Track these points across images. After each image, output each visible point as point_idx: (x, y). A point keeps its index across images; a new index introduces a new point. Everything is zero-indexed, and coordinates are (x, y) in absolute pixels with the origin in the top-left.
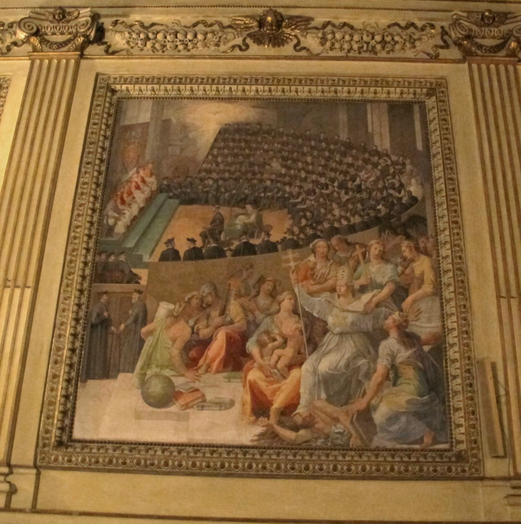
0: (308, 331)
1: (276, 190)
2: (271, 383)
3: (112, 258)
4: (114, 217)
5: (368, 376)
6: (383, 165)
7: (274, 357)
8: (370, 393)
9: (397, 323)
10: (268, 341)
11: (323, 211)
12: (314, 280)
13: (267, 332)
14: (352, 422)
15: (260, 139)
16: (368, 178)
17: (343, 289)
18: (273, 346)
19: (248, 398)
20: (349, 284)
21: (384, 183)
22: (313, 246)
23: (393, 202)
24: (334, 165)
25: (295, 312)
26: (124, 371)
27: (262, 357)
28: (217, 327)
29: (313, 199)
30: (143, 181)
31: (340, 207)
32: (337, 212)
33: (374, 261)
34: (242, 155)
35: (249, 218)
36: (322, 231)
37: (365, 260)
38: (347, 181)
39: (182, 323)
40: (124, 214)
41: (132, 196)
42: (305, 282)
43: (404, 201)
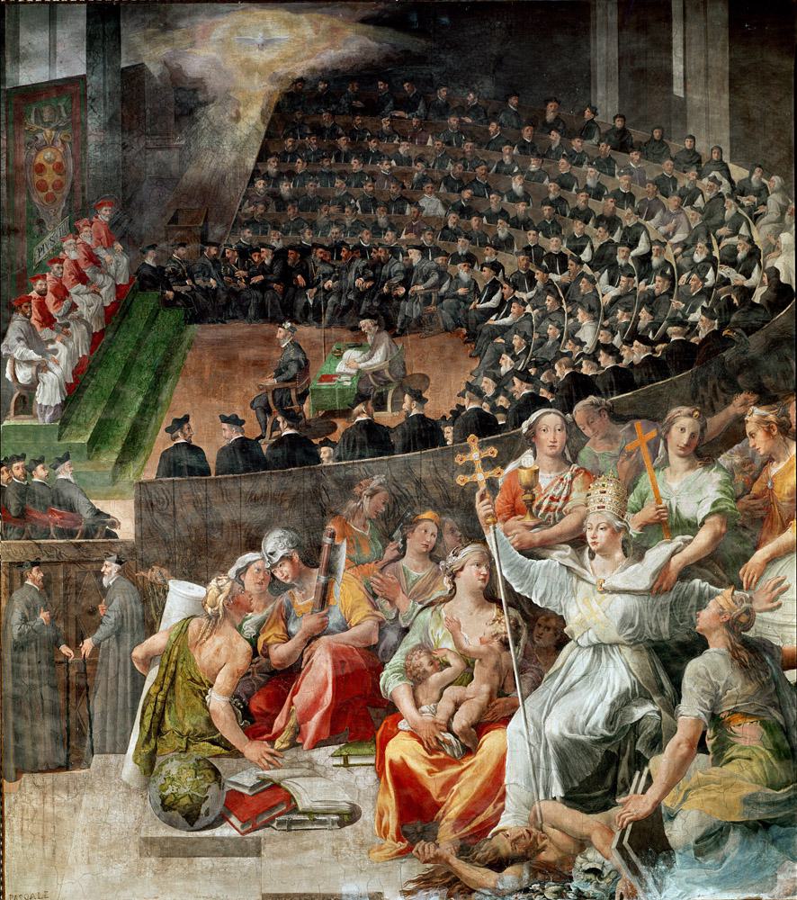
0: (521, 642)
1: (434, 278)
2: (441, 765)
3: (40, 473)
4: (30, 363)
5: (657, 743)
6: (708, 195)
7: (446, 705)
8: (660, 780)
9: (728, 617)
10: (429, 669)
11: (551, 330)
12: (533, 516)
13: (425, 647)
14: (620, 848)
15: (385, 124)
16: (667, 236)
17: (602, 536)
18: (443, 680)
19: (390, 801)
20: (618, 523)
21: (710, 246)
22: (530, 427)
23: (729, 298)
24: (581, 200)
25: (489, 596)
26: (102, 752)
27: (417, 705)
28: (311, 639)
29: (530, 300)
30: (93, 259)
31: (596, 319)
32: (588, 334)
33: (676, 461)
34: (342, 175)
35: (371, 356)
36: (552, 390)
37: (657, 461)
38: (617, 245)
39: (228, 628)
40: (55, 351)
41: (67, 302)
42: (512, 522)
43: (757, 299)
